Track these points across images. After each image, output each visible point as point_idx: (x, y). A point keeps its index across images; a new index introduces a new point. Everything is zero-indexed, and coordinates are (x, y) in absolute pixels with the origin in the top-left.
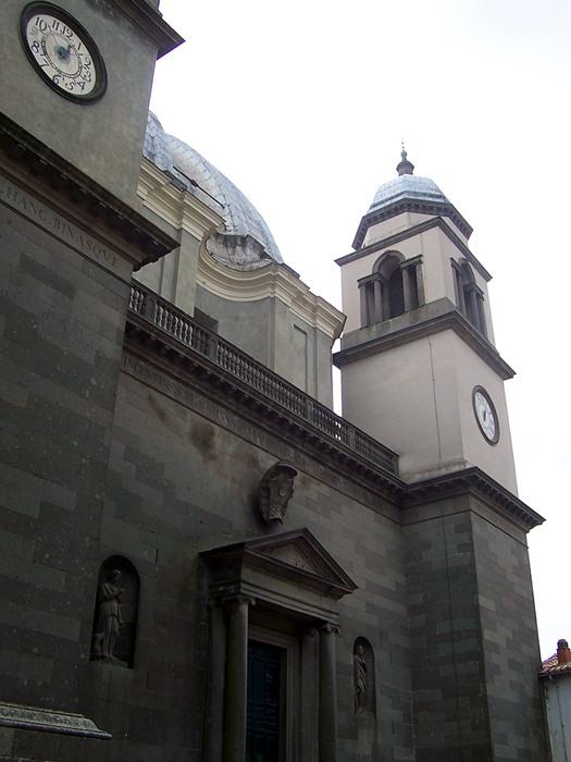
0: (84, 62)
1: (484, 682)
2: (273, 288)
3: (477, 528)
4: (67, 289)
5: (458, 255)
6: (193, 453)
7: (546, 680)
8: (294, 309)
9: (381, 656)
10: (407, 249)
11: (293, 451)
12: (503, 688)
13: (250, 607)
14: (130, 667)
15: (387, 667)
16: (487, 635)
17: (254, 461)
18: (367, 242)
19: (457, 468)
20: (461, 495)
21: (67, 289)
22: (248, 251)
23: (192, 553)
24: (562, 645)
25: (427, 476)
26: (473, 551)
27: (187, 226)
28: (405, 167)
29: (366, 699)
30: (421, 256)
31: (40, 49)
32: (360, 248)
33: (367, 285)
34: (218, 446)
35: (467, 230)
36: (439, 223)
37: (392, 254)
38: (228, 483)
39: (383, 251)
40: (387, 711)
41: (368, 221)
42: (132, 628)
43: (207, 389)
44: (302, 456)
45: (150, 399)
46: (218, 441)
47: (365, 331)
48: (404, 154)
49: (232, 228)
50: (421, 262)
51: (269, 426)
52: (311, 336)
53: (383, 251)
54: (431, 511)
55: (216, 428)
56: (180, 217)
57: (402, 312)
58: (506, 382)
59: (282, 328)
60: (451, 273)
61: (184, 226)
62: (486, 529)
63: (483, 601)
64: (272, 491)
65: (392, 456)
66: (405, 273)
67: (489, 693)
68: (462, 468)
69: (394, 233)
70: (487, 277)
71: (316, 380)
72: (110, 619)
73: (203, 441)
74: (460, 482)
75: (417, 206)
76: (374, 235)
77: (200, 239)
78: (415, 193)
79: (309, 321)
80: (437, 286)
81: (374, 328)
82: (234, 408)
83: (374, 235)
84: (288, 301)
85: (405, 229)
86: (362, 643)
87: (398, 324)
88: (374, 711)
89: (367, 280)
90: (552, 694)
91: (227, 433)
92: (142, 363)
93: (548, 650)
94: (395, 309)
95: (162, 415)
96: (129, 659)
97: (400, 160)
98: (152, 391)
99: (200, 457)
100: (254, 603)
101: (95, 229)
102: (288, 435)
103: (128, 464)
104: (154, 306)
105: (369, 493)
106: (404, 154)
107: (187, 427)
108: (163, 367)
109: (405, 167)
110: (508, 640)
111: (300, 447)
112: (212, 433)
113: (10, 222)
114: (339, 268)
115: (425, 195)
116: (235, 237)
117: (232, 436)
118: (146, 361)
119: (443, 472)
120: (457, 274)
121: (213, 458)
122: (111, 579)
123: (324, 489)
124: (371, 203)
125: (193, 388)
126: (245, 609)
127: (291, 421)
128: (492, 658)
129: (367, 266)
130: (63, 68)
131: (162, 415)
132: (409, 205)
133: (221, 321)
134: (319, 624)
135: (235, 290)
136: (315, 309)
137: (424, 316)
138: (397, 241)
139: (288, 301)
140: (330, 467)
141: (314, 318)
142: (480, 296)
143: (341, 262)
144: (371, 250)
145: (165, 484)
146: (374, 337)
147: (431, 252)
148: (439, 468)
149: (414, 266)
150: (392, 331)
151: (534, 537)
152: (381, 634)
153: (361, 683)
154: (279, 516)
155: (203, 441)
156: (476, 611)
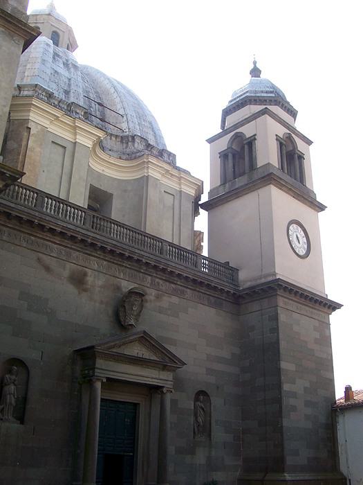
1: (281, 417)
2: (148, 170)
3: (282, 317)
5: (282, 131)
6: (71, 289)
7: (335, 411)
9: (217, 402)
10: (247, 131)
11: (149, 278)
12: (297, 418)
13: (102, 383)
14: (22, 423)
15: (220, 407)
16: (286, 387)
17: (118, 288)
18: (227, 125)
19: (271, 278)
20: (272, 296)
22: (136, 145)
23: (68, 351)
24: (348, 390)
25: (253, 283)
26: (278, 333)
27: (81, 139)
28: (255, 72)
29: (204, 429)
30: (255, 135)
32: (225, 132)
33: (224, 156)
34: (90, 282)
35: (293, 113)
37: (239, 135)
38: (97, 304)
39: (233, 133)
40: (219, 435)
41: (227, 113)
42: (23, 401)
43: (81, 248)
44: (157, 280)
45: (39, 259)
46: (90, 279)
47: (222, 187)
48: (255, 63)
49: (127, 130)
50: (255, 139)
51: (129, 265)
52: (177, 197)
53: (233, 133)
54: (255, 306)
55: (89, 272)
56: (75, 134)
58: (319, 213)
59: (153, 194)
61: (77, 140)
62: (290, 316)
63: (284, 365)
64: (127, 307)
65: (235, 271)
66: (246, 147)
67: (284, 425)
68: (274, 278)
69: (241, 120)
70: (309, 142)
71: (180, 225)
72: (8, 396)
73: (79, 280)
74: (270, 288)
75: (255, 100)
77: (90, 146)
78: (256, 92)
80: (268, 155)
81: (227, 185)
82: (102, 257)
84: (157, 176)
85: (247, 117)
86: (202, 395)
87: (241, 182)
88: (210, 435)
89: (224, 153)
90: (340, 419)
91: (97, 273)
93: (339, 394)
95: (48, 269)
96: (21, 419)
98: (40, 255)
99: (76, 291)
100: (104, 380)
102: (145, 268)
103: (22, 302)
104: (43, 200)
105: (211, 298)
106: (255, 63)
107: (66, 273)
108: (47, 238)
109: (255, 72)
110: (305, 388)
111: (155, 275)
112: (85, 274)
114: (209, 145)
115: (262, 92)
116: (127, 137)
117: (101, 274)
118: (35, 236)
119: (263, 281)
120: (281, 145)
121: (85, 290)
122: (10, 372)
123: (175, 300)
124: (231, 99)
125: (71, 248)
126: (98, 385)
127: (144, 260)
128: (288, 402)
129: (224, 144)
131: (48, 269)
132: (250, 100)
133: (115, 194)
134: (157, 389)
135: (123, 172)
136: (180, 178)
137: (256, 175)
138: (242, 125)
141: (180, 185)
142: (301, 157)
143: (210, 141)
144: (230, 130)
145: (49, 311)
146: (227, 190)
148: (261, 279)
149: (251, 142)
150: (237, 187)
151: (335, 318)
152: (218, 388)
153: (200, 420)
154: (132, 322)
155: (79, 280)
156: (278, 371)
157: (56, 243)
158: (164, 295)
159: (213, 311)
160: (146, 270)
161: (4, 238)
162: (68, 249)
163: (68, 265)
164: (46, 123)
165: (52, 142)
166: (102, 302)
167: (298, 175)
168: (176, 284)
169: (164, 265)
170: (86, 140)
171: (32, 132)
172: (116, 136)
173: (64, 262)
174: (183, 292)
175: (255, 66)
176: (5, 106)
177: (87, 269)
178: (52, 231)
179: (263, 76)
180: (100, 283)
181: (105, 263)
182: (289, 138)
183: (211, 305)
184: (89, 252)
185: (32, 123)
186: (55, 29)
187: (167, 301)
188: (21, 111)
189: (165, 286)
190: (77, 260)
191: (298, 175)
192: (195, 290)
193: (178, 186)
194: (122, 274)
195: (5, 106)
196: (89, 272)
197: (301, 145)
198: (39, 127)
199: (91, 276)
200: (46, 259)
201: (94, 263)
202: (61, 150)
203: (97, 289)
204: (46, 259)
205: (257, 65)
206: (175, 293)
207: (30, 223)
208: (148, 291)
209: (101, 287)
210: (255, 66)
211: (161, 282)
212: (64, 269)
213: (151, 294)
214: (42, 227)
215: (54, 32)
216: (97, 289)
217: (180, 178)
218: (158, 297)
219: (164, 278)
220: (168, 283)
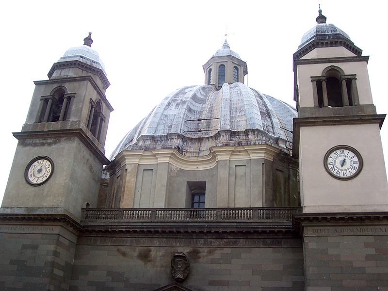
0: (47, 167)
4: (35, 247)
6: (140, 263)
8: (235, 158)
11: (203, 240)
21: (35, 247)
28: (321, 19)
31: (33, 176)
34: (153, 256)
38: (159, 268)
44: (209, 240)
46: (153, 254)
48: (320, 12)
55: (153, 249)
73: (145, 256)
79: (246, 157)
91: (158, 248)
92: (114, 238)
95: (124, 254)
98: (119, 247)
101: (43, 224)
103: (108, 277)
105: (268, 240)
106: (320, 12)
107: (136, 254)
109: (321, 19)
112: (150, 251)
113: (19, 237)
121: (150, 261)
125: (139, 237)
130: (40, 175)
131: (124, 254)
136: (246, 151)
139: (227, 157)
140: (230, 238)
142: (350, 80)
145: (125, 279)
155: (145, 256)
157: (128, 237)
158: (217, 250)
159: (270, 250)
160: (197, 236)
161: (98, 244)
162: (137, 239)
163: (137, 249)
164: (136, 161)
165: (144, 170)
166: (162, 266)
168: (227, 238)
169: (215, 228)
170: (164, 159)
171: (128, 171)
172: (211, 137)
173: (133, 248)
174: (235, 242)
176: (66, 180)
177: (150, 248)
178: (121, 232)
179: (328, 22)
180: (161, 254)
181: (164, 239)
183: (266, 245)
184: (151, 236)
185: (128, 165)
186: (220, 64)
187: (218, 254)
188: (122, 161)
189: (216, 243)
190: (144, 243)
192: (248, 238)
193: (248, 156)
194: (178, 243)
195: (66, 180)
196: (153, 249)
198: (133, 165)
199: (153, 251)
200: (123, 249)
201: (156, 242)
202: (150, 172)
203: (158, 258)
204: (123, 249)
205: (323, 14)
206: (227, 245)
207: (107, 232)
208: (201, 250)
209: (163, 256)
211: (213, 240)
212: (135, 251)
213: (204, 251)
214: (114, 232)
215: (220, 66)
216: (158, 258)
217: (246, 151)
218: (210, 252)
219: (214, 237)
220: (220, 240)
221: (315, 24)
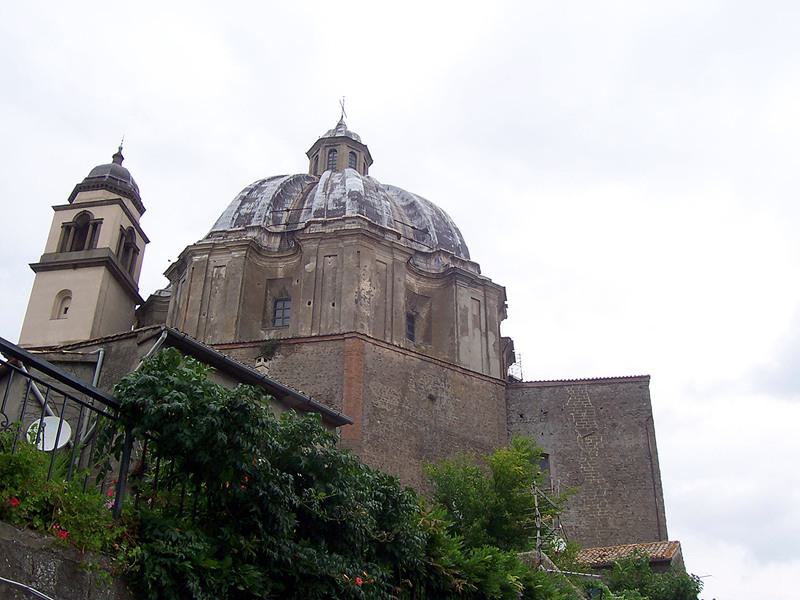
5: (127, 224)
10: (97, 213)
28: (118, 157)
33: (66, 227)
35: (141, 210)
36: (119, 202)
39: (82, 210)
41: (79, 189)
48: (121, 149)
53: (82, 210)
57: (82, 249)
60: (117, 233)
70: (147, 241)
76: (82, 197)
80: (107, 239)
83: (82, 197)
87: (75, 256)
94: (78, 246)
97: (117, 151)
106: (121, 149)
109: (118, 157)
120: (122, 235)
129: (70, 216)
142: (136, 251)
143: (56, 208)
147: (111, 222)
149: (97, 224)
167: (129, 262)
175: (120, 152)
182: (131, 231)
191: (129, 262)
197: (139, 240)
205: (122, 153)
210: (120, 152)
221: (109, 161)
